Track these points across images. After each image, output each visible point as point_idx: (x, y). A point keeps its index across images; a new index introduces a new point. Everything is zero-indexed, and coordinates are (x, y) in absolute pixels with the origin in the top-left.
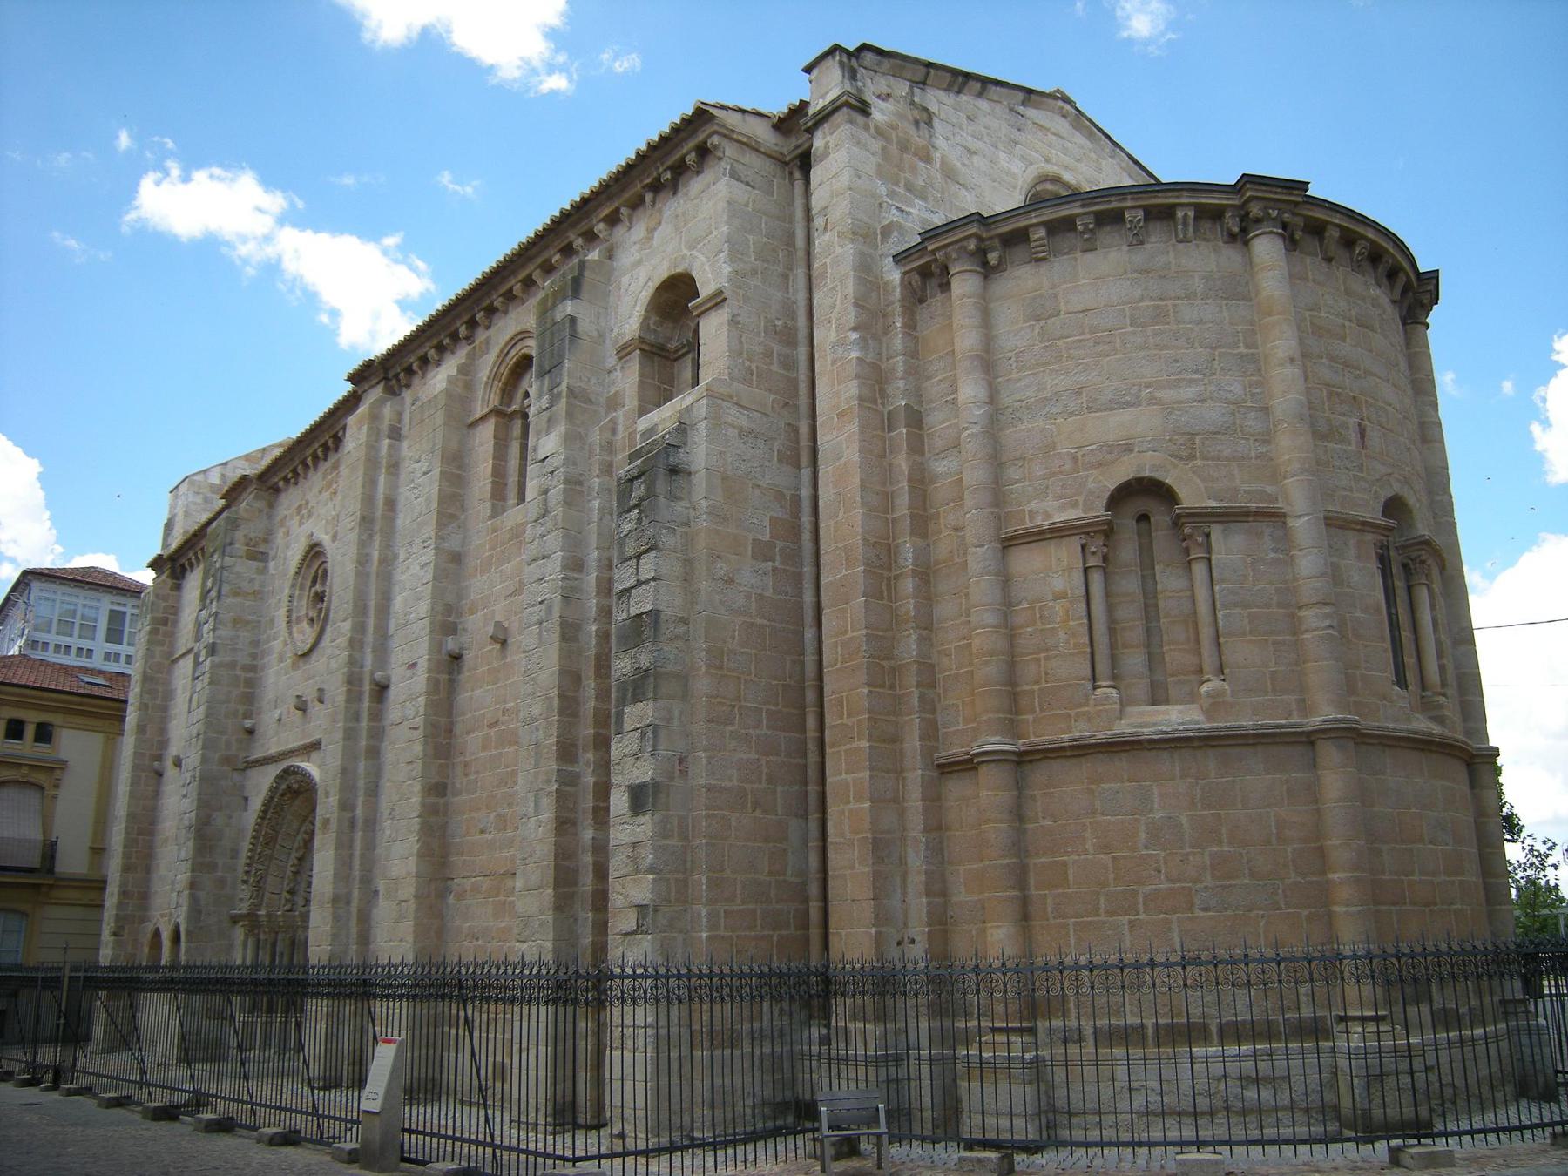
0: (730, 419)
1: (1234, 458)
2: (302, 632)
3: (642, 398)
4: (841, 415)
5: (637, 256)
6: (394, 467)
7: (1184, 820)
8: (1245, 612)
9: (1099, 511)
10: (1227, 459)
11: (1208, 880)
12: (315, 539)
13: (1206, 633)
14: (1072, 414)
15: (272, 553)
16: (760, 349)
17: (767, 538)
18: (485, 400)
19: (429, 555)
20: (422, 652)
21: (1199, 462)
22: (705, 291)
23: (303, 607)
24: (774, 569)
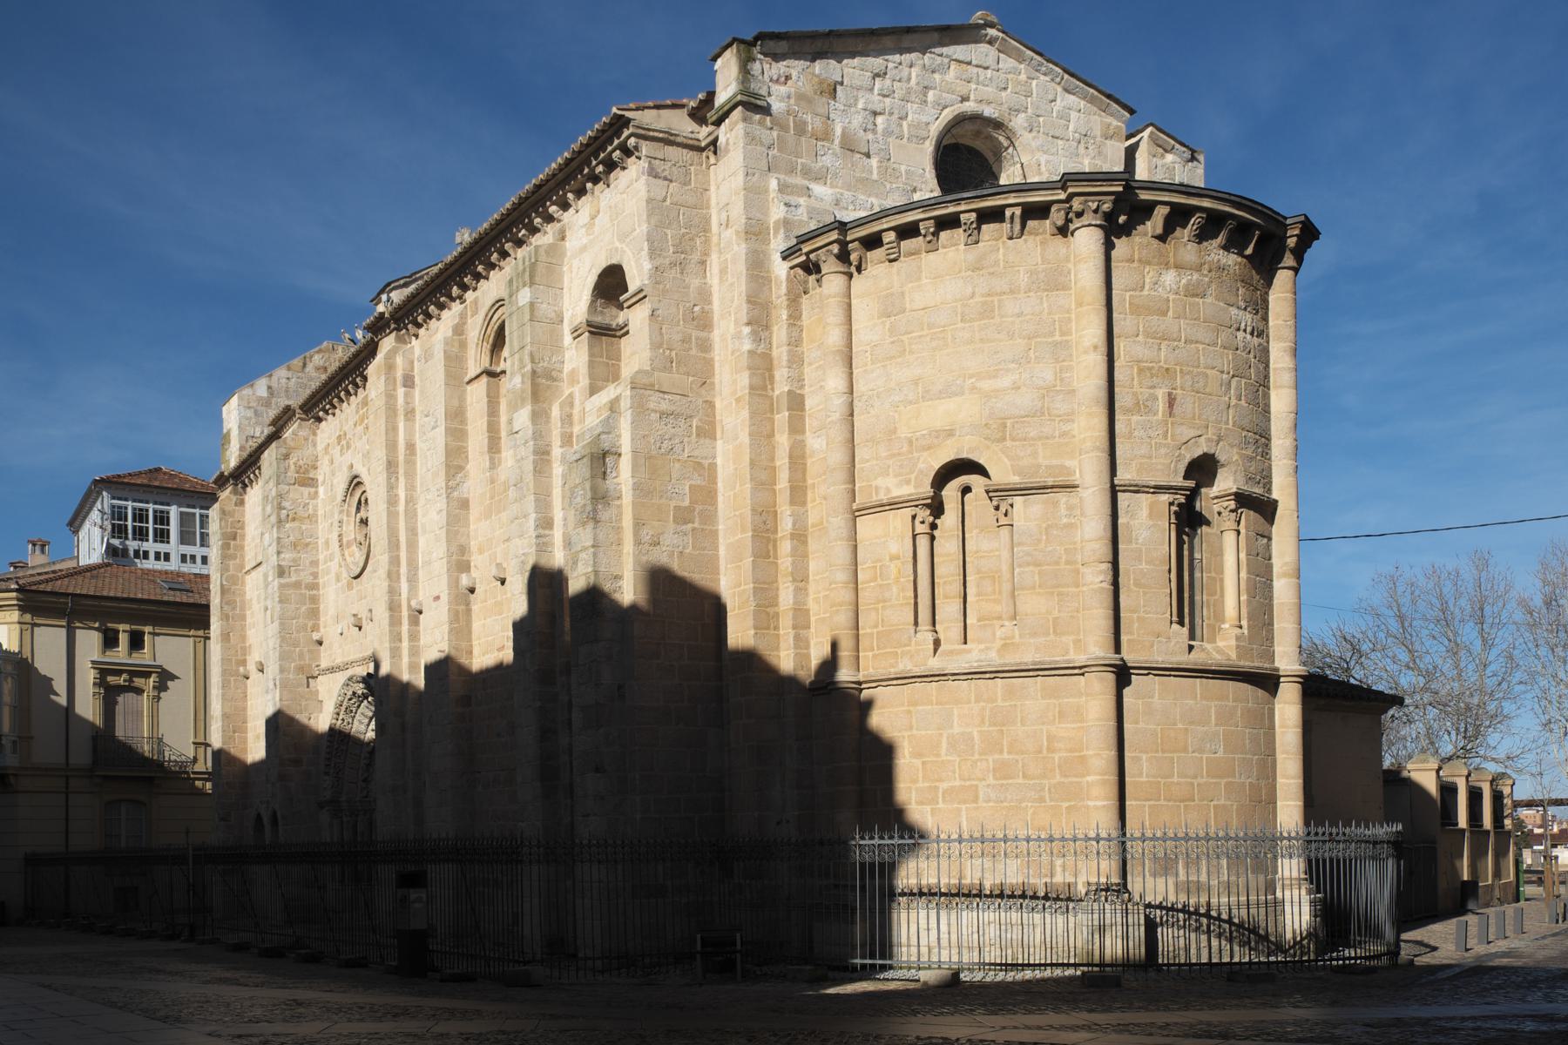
0: (652, 405)
2: (352, 555)
3: (591, 376)
4: (738, 400)
5: (585, 241)
6: (410, 414)
8: (1036, 570)
11: (991, 780)
12: (355, 472)
13: (1007, 587)
15: (321, 479)
16: (678, 337)
17: (687, 503)
18: (476, 360)
19: (442, 504)
20: (442, 586)
22: (632, 288)
23: (351, 530)
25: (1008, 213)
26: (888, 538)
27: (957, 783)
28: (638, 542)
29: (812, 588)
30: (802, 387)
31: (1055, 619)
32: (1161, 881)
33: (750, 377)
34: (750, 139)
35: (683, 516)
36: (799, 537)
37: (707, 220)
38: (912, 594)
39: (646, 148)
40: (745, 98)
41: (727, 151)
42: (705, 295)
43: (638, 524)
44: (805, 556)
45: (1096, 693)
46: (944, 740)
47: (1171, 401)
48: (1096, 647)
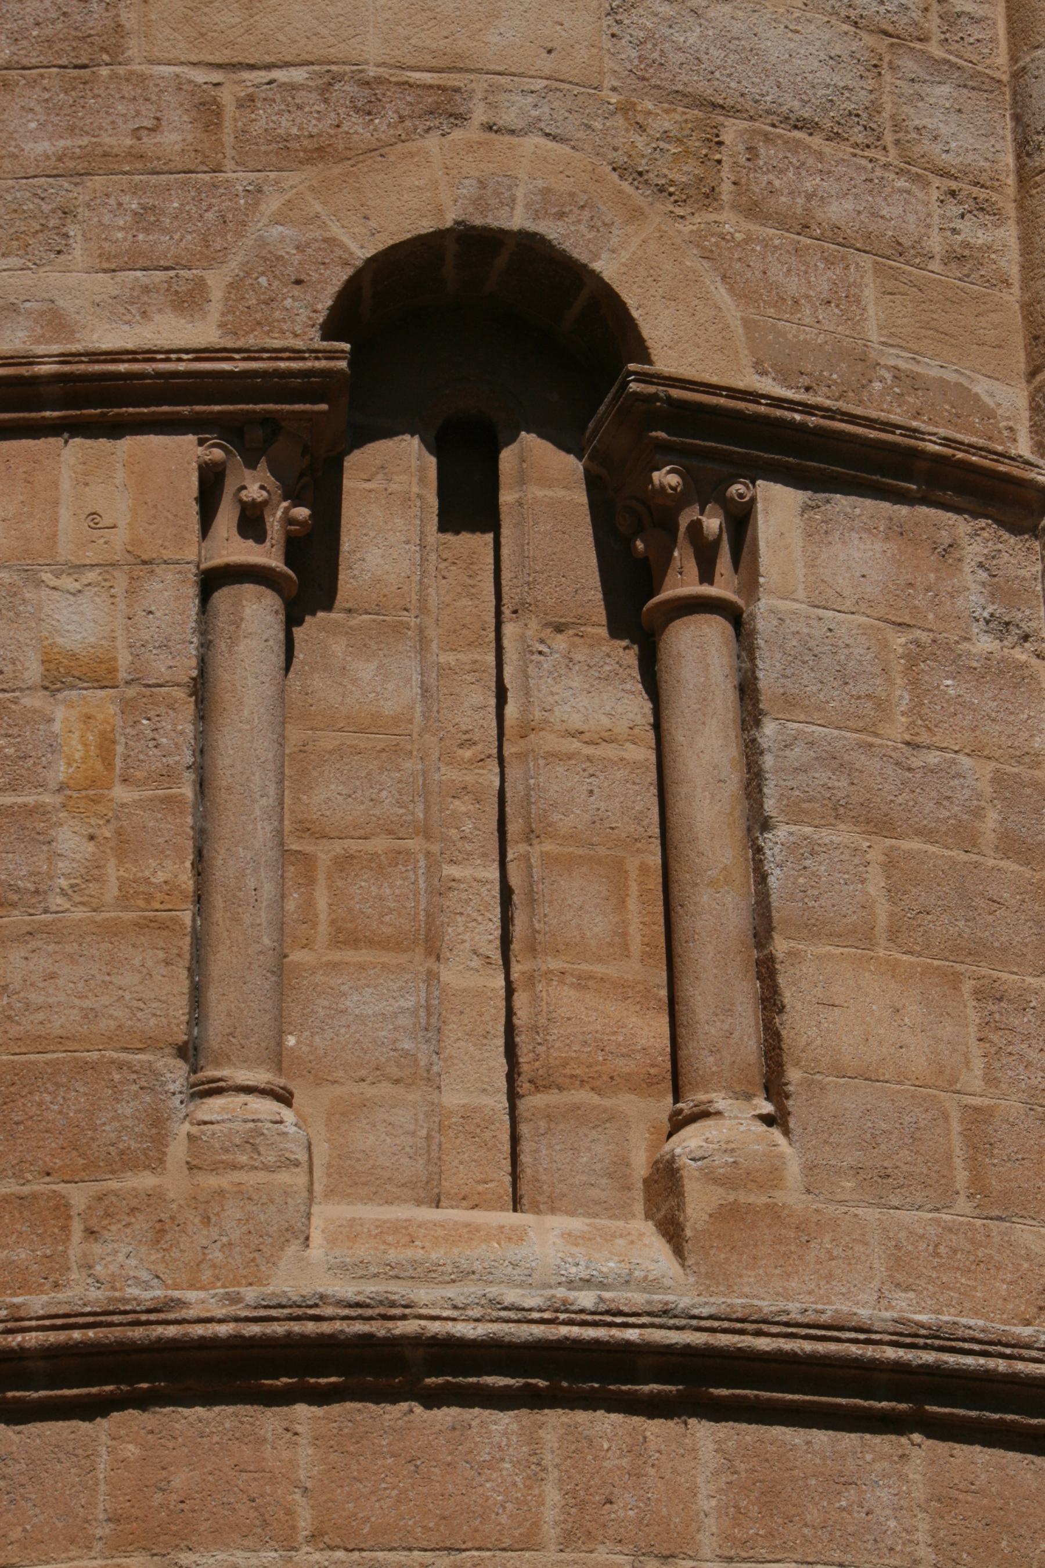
8: (877, 849)
9: (296, 327)
10: (837, 236)
21: (730, 222)
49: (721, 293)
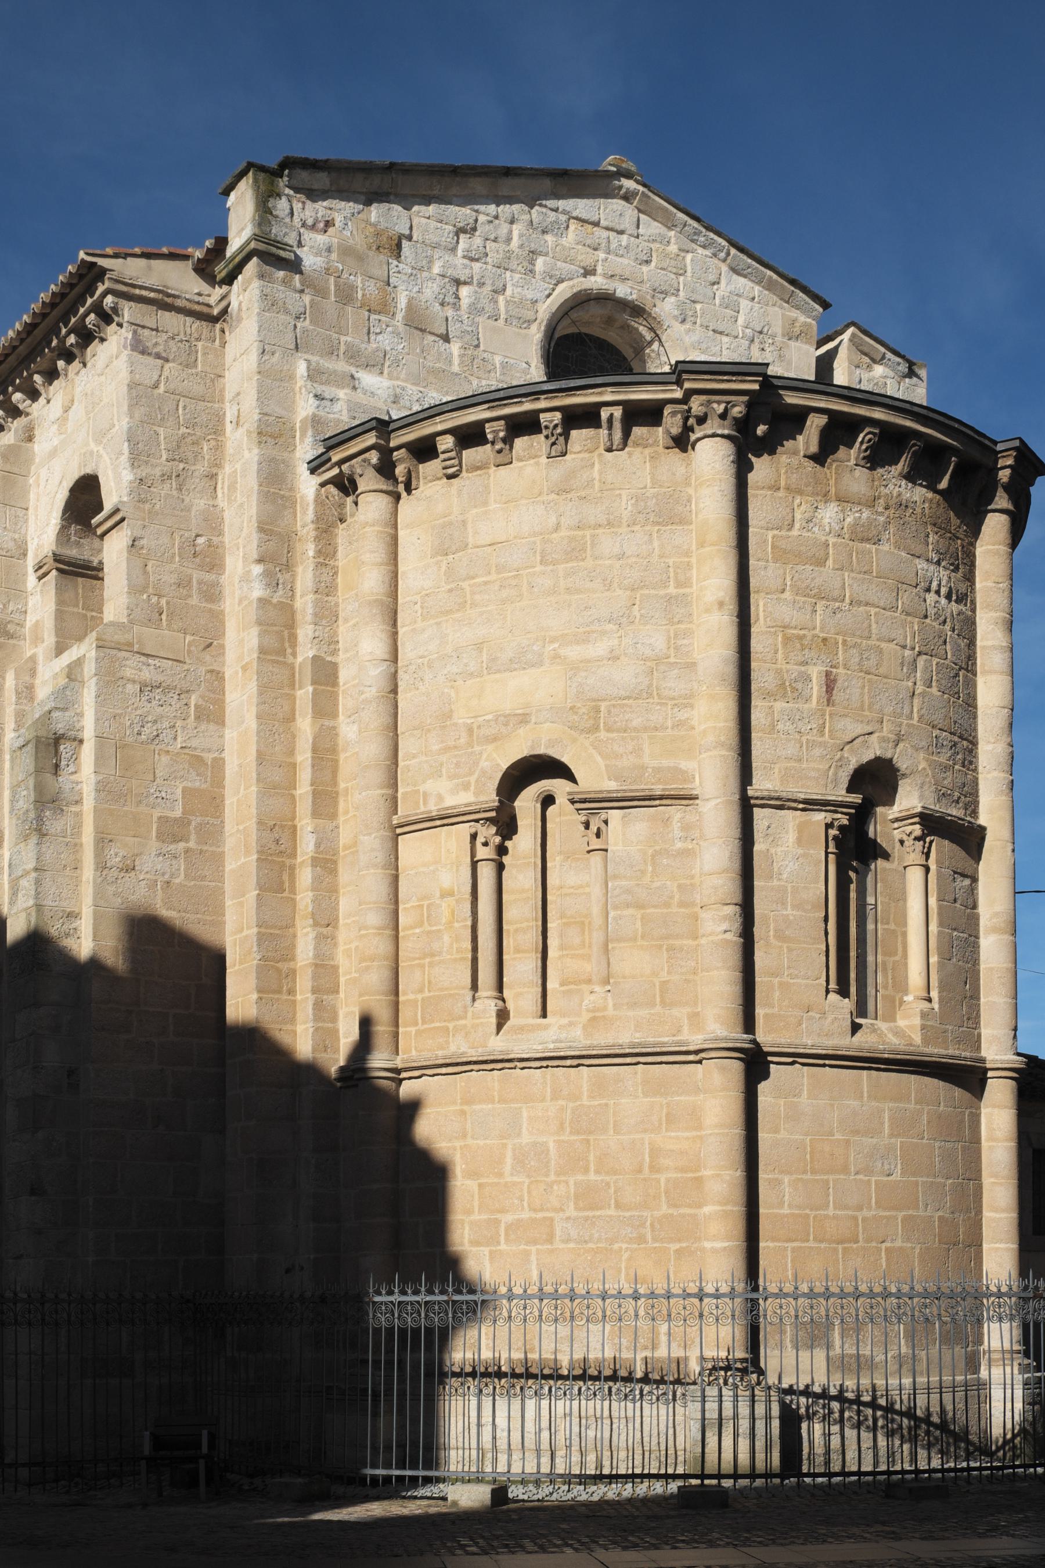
0: (128, 673)
1: (646, 729)
4: (245, 668)
7: (551, 1145)
8: (639, 914)
11: (571, 1211)
13: (598, 937)
14: (472, 675)
16: (172, 579)
17: (178, 813)
21: (603, 734)
22: (108, 506)
24: (187, 851)
25: (604, 414)
26: (438, 864)
27: (526, 1215)
28: (101, 866)
29: (342, 935)
30: (335, 652)
31: (664, 983)
32: (805, 1355)
33: (260, 635)
34: (269, 303)
35: (172, 831)
36: (326, 863)
37: (220, 418)
38: (468, 945)
39: (128, 311)
40: (262, 247)
41: (240, 320)
42: (213, 522)
43: (102, 841)
44: (333, 890)
45: (718, 1086)
46: (509, 1154)
47: (830, 684)
48: (715, 1022)
49: (599, 759)
